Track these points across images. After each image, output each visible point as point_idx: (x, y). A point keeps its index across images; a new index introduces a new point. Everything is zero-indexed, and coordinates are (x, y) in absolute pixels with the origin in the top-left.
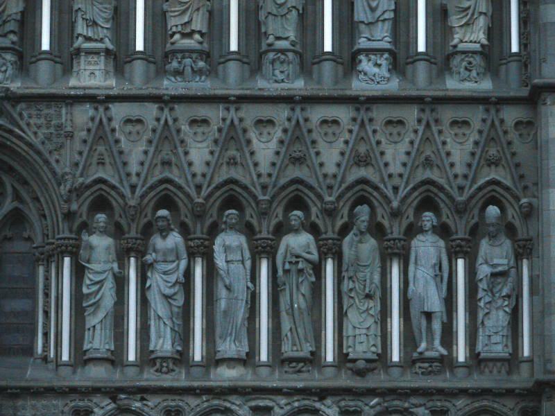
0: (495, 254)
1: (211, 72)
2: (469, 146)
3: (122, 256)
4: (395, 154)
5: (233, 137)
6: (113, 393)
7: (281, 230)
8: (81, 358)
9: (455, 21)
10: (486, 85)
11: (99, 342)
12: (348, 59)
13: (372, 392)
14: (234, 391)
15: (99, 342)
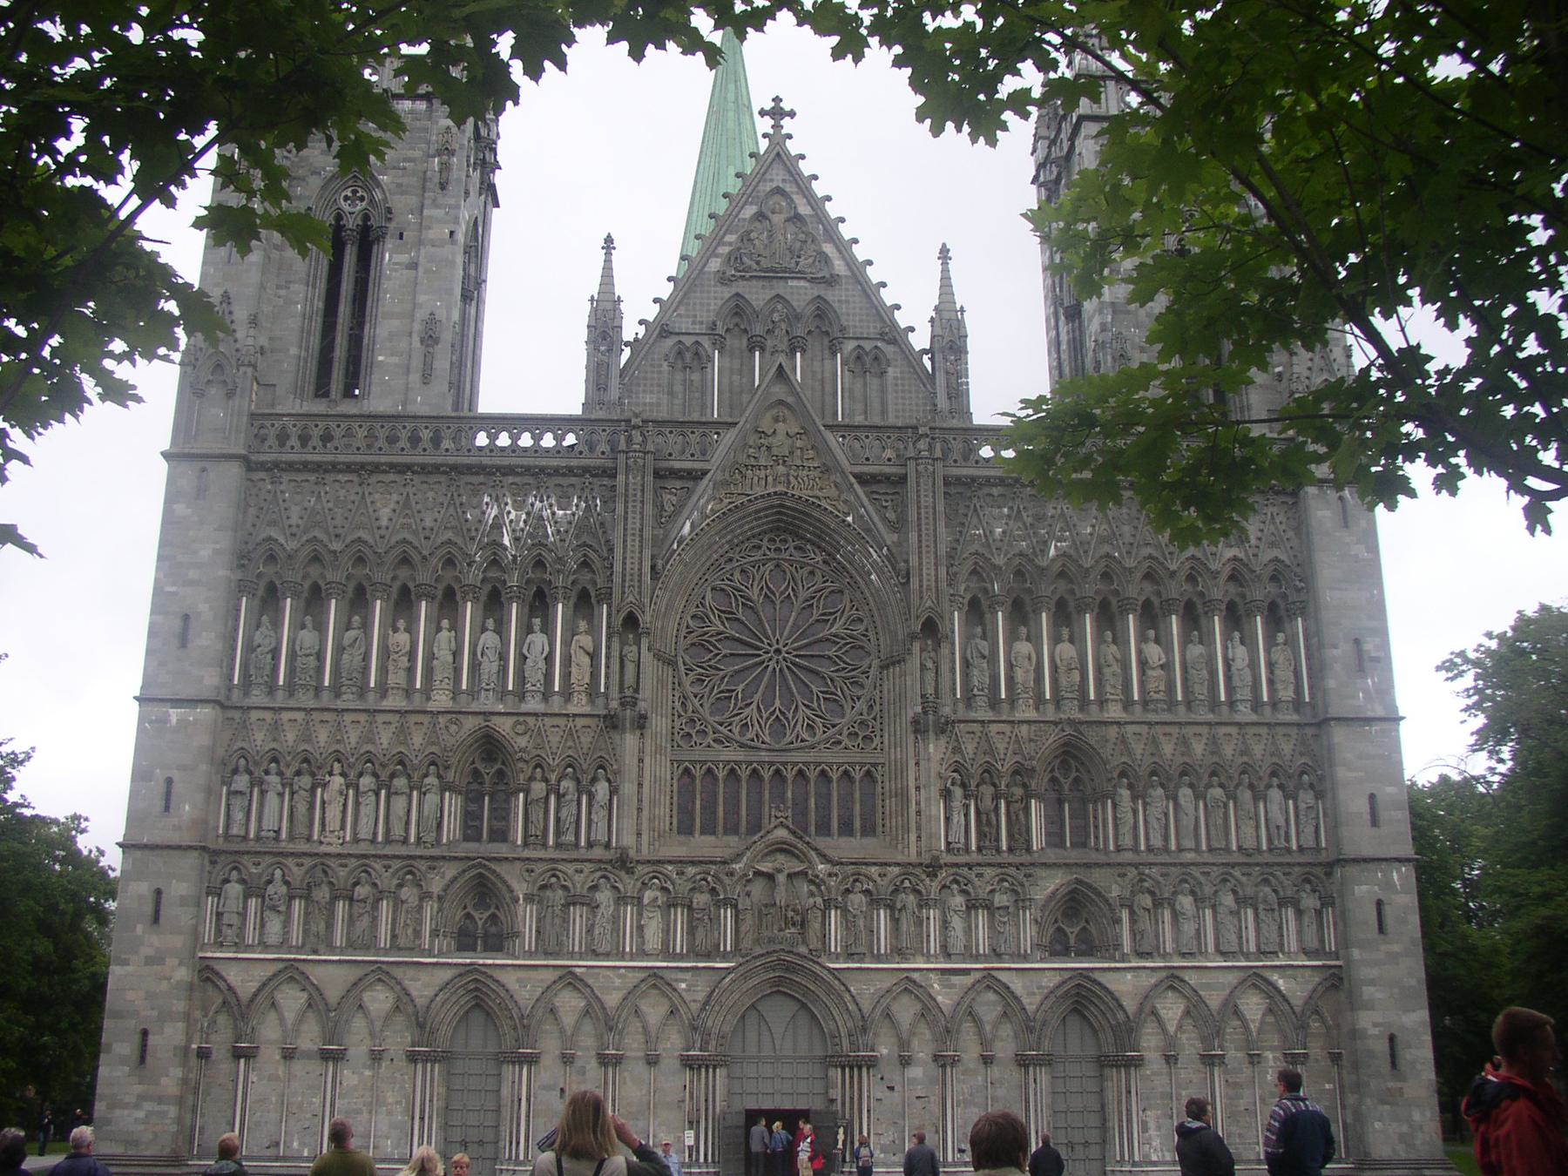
0: (1307, 798)
1: (1169, 710)
2: (1292, 747)
3: (1134, 798)
4: (1258, 750)
5: (1184, 742)
6: (1136, 866)
7: (1209, 786)
8: (1119, 849)
9: (1279, 686)
10: (1295, 718)
11: (1127, 841)
12: (1232, 703)
13: (1257, 864)
14: (1193, 864)
15: (1127, 841)
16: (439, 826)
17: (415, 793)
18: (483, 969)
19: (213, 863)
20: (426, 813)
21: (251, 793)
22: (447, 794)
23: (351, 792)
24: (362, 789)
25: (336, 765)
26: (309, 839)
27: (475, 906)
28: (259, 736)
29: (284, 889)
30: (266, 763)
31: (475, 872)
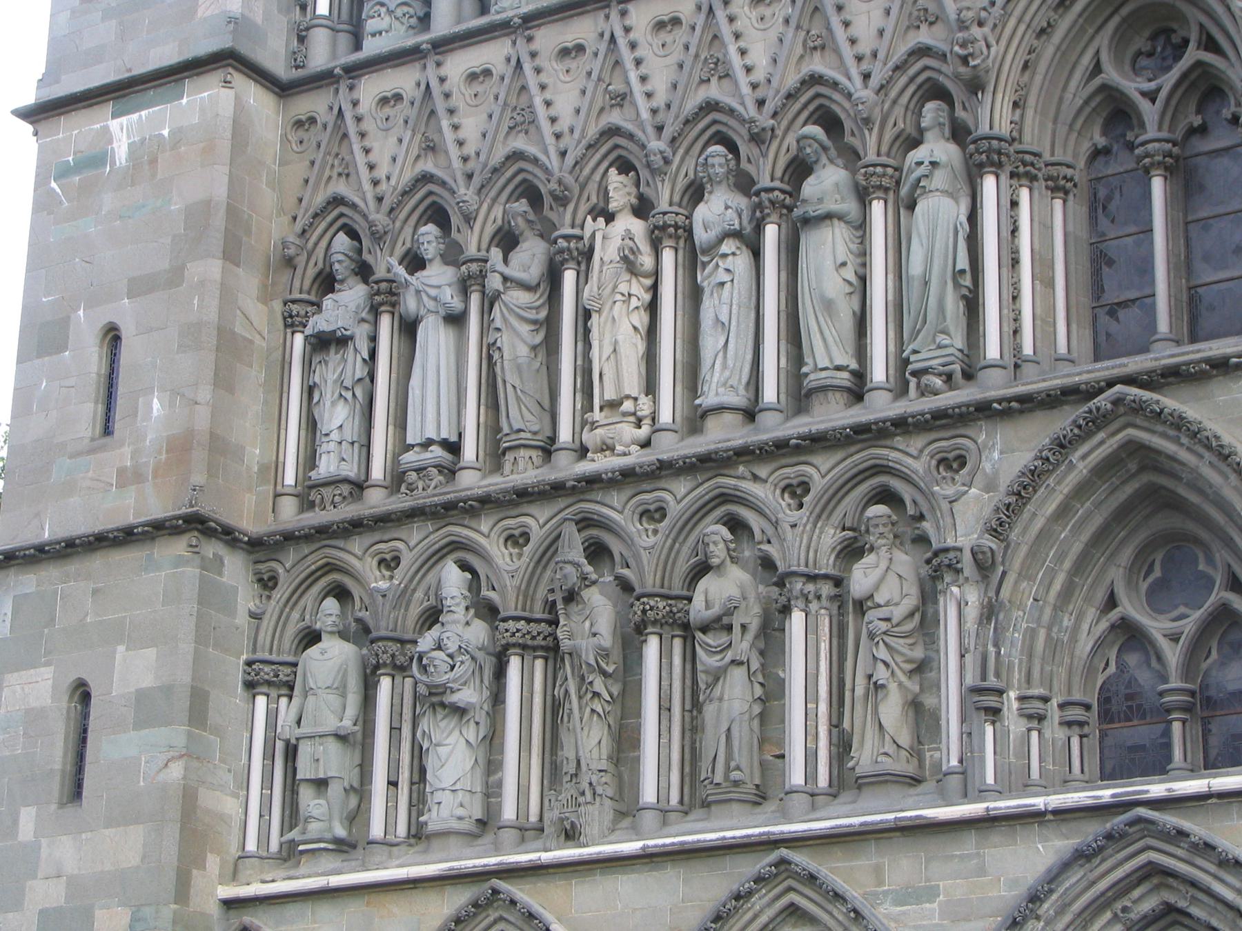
16: (973, 305)
17: (877, 208)
18: (1170, 819)
19: (267, 583)
20: (916, 265)
21: (374, 339)
22: (989, 185)
23: (668, 257)
24: (701, 236)
25: (614, 176)
26: (548, 449)
27: (1157, 598)
28: (384, 148)
29: (478, 632)
30: (408, 230)
31: (1103, 445)
